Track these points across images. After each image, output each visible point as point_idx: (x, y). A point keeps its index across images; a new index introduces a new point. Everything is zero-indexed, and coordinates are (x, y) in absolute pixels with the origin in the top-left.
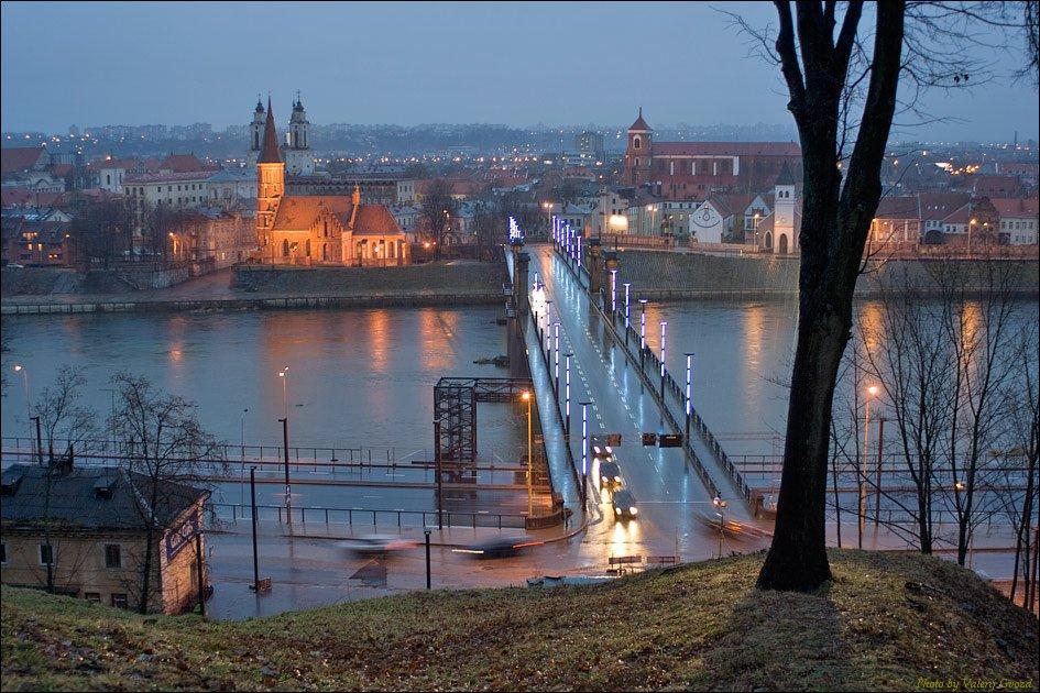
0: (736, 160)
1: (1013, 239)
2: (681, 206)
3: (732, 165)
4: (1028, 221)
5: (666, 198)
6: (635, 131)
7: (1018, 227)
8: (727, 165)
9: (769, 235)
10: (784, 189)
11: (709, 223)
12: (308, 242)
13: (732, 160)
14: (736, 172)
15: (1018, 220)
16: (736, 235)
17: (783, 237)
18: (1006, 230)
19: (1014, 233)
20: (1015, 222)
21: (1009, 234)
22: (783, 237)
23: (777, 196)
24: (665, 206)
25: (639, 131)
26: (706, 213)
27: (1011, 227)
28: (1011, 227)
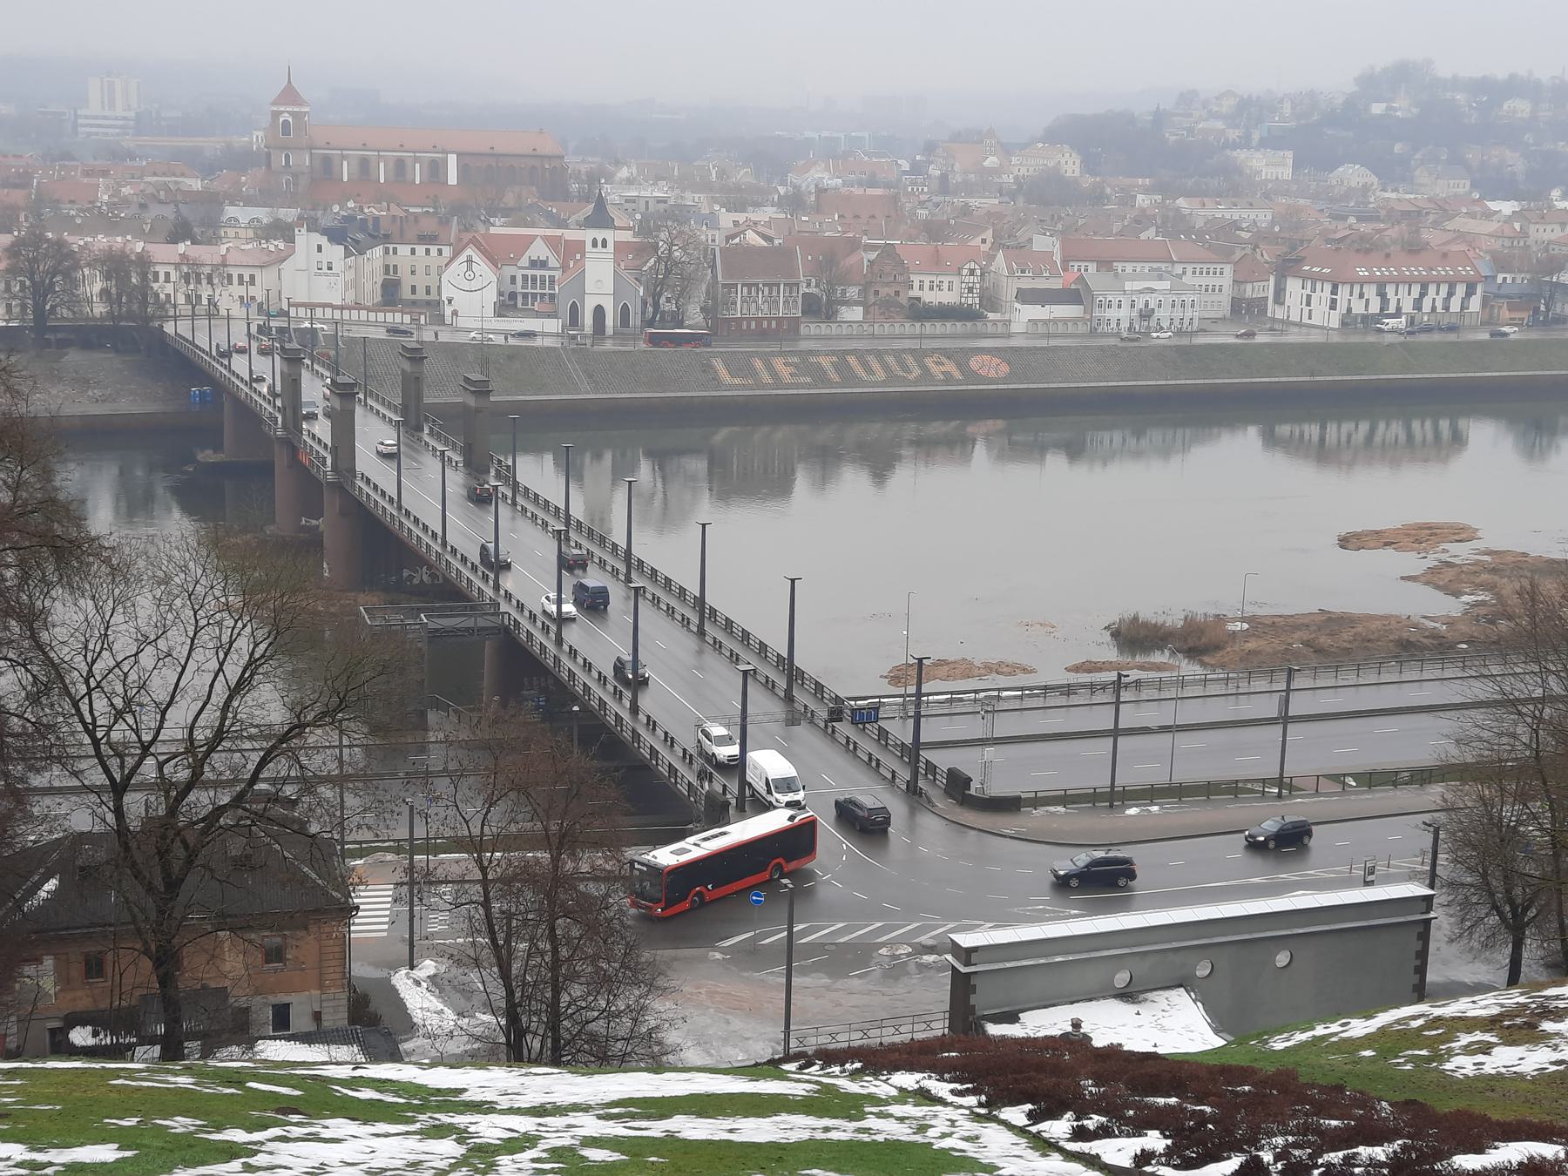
0: (452, 160)
2: (413, 252)
4: (946, 279)
5: (387, 238)
7: (931, 288)
10: (600, 234)
11: (475, 285)
13: (446, 161)
14: (452, 179)
15: (933, 278)
16: (507, 304)
17: (599, 312)
20: (927, 279)
22: (599, 312)
23: (589, 247)
24: (387, 251)
26: (469, 268)
27: (921, 288)
28: (921, 288)
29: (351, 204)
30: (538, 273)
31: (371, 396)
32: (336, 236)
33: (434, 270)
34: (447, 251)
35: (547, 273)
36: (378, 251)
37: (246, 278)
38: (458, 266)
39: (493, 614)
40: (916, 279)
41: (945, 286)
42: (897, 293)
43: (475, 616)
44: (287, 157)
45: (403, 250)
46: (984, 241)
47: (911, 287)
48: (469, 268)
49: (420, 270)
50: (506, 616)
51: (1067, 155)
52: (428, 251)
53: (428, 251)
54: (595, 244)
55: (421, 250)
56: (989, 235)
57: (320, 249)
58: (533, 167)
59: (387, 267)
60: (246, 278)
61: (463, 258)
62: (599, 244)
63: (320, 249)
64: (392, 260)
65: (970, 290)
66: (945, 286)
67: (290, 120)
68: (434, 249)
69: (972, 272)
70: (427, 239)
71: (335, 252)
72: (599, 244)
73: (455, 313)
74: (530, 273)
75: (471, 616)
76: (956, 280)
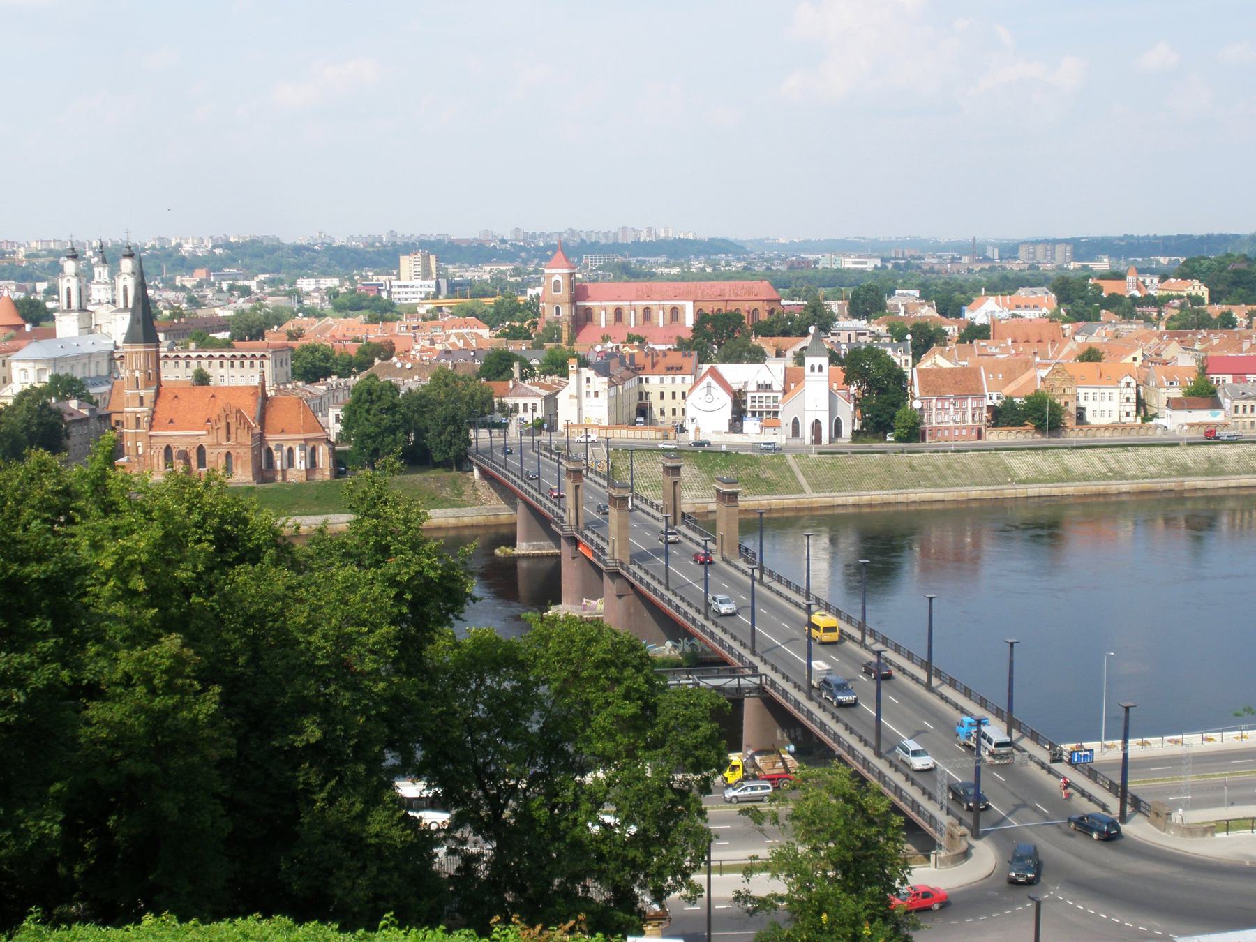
1: (1089, 417)
3: (684, 313)
4: (1107, 391)
6: (554, 271)
8: (675, 313)
9: (795, 422)
12: (201, 450)
13: (683, 307)
14: (689, 321)
17: (817, 425)
18: (1082, 403)
19: (1090, 407)
20: (1091, 391)
21: (1084, 409)
22: (817, 425)
25: (560, 271)
26: (709, 393)
29: (610, 345)
30: (764, 394)
31: (637, 498)
32: (602, 370)
33: (679, 396)
34: (690, 379)
35: (771, 395)
36: (634, 382)
37: (530, 407)
38: (699, 392)
39: (752, 676)
40: (1081, 391)
41: (1107, 396)
42: (1066, 404)
43: (739, 677)
44: (558, 309)
45: (654, 380)
46: (1135, 359)
47: (1078, 399)
48: (709, 393)
49: (668, 396)
50: (764, 677)
51: (1196, 288)
52: (674, 380)
53: (674, 380)
54: (813, 369)
55: (668, 379)
56: (1138, 354)
57: (588, 381)
58: (756, 309)
59: (641, 394)
60: (530, 407)
61: (704, 384)
62: (817, 369)
63: (588, 381)
64: (646, 387)
65: (1128, 400)
66: (1107, 396)
67: (561, 280)
68: (679, 378)
69: (1128, 385)
70: (673, 369)
71: (600, 383)
72: (817, 369)
73: (698, 430)
74: (757, 395)
75: (733, 677)
76: (1115, 392)
